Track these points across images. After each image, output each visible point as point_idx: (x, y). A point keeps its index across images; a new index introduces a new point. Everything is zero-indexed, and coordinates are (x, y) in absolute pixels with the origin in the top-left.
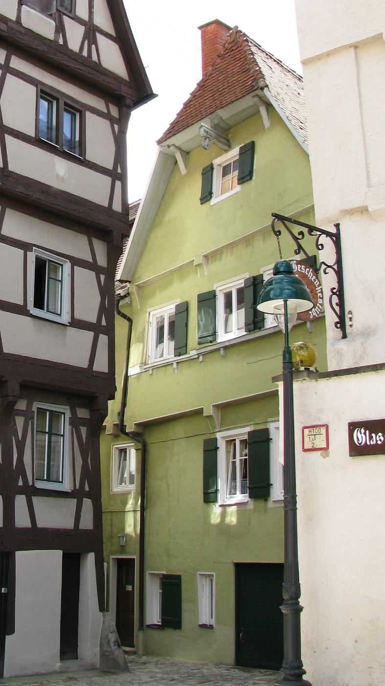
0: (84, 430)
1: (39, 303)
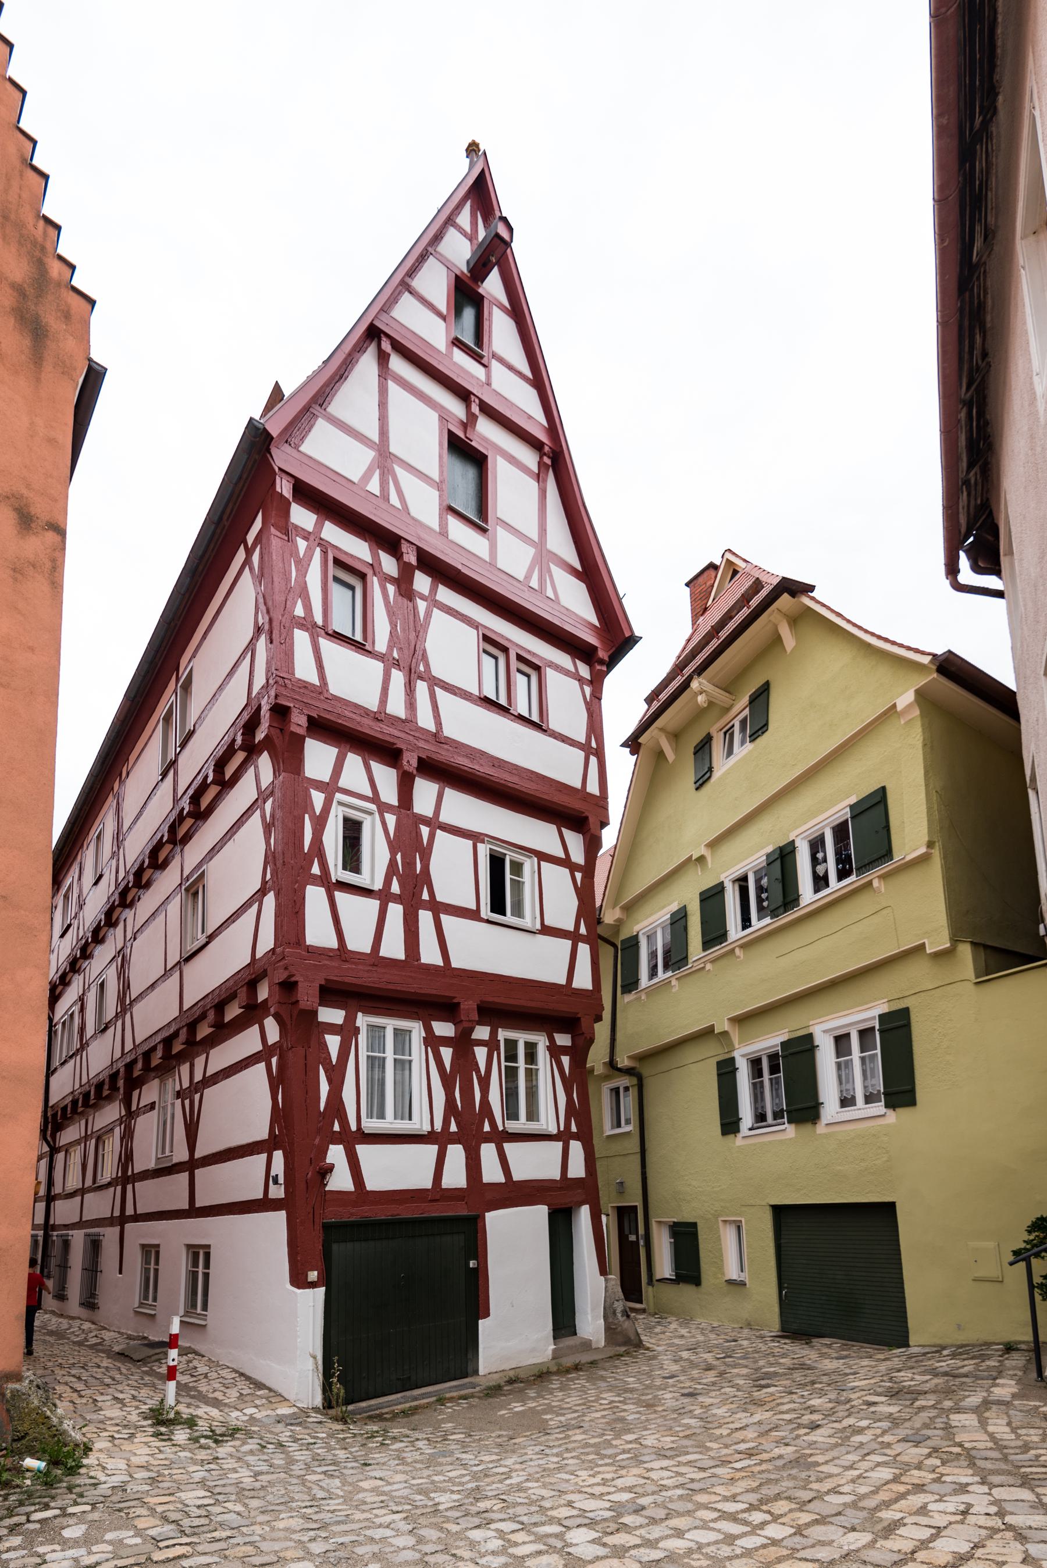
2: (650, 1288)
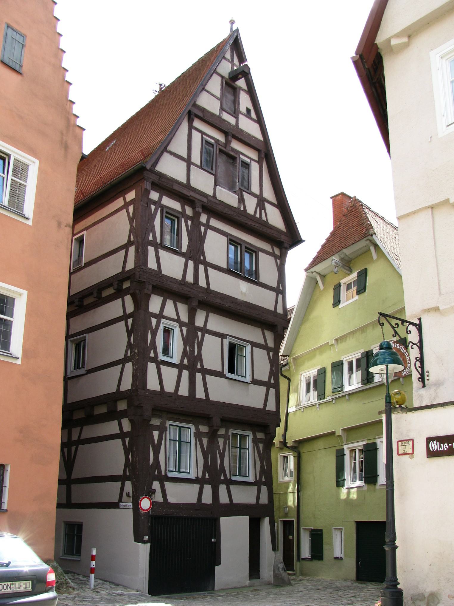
0: (261, 446)
1: (231, 370)
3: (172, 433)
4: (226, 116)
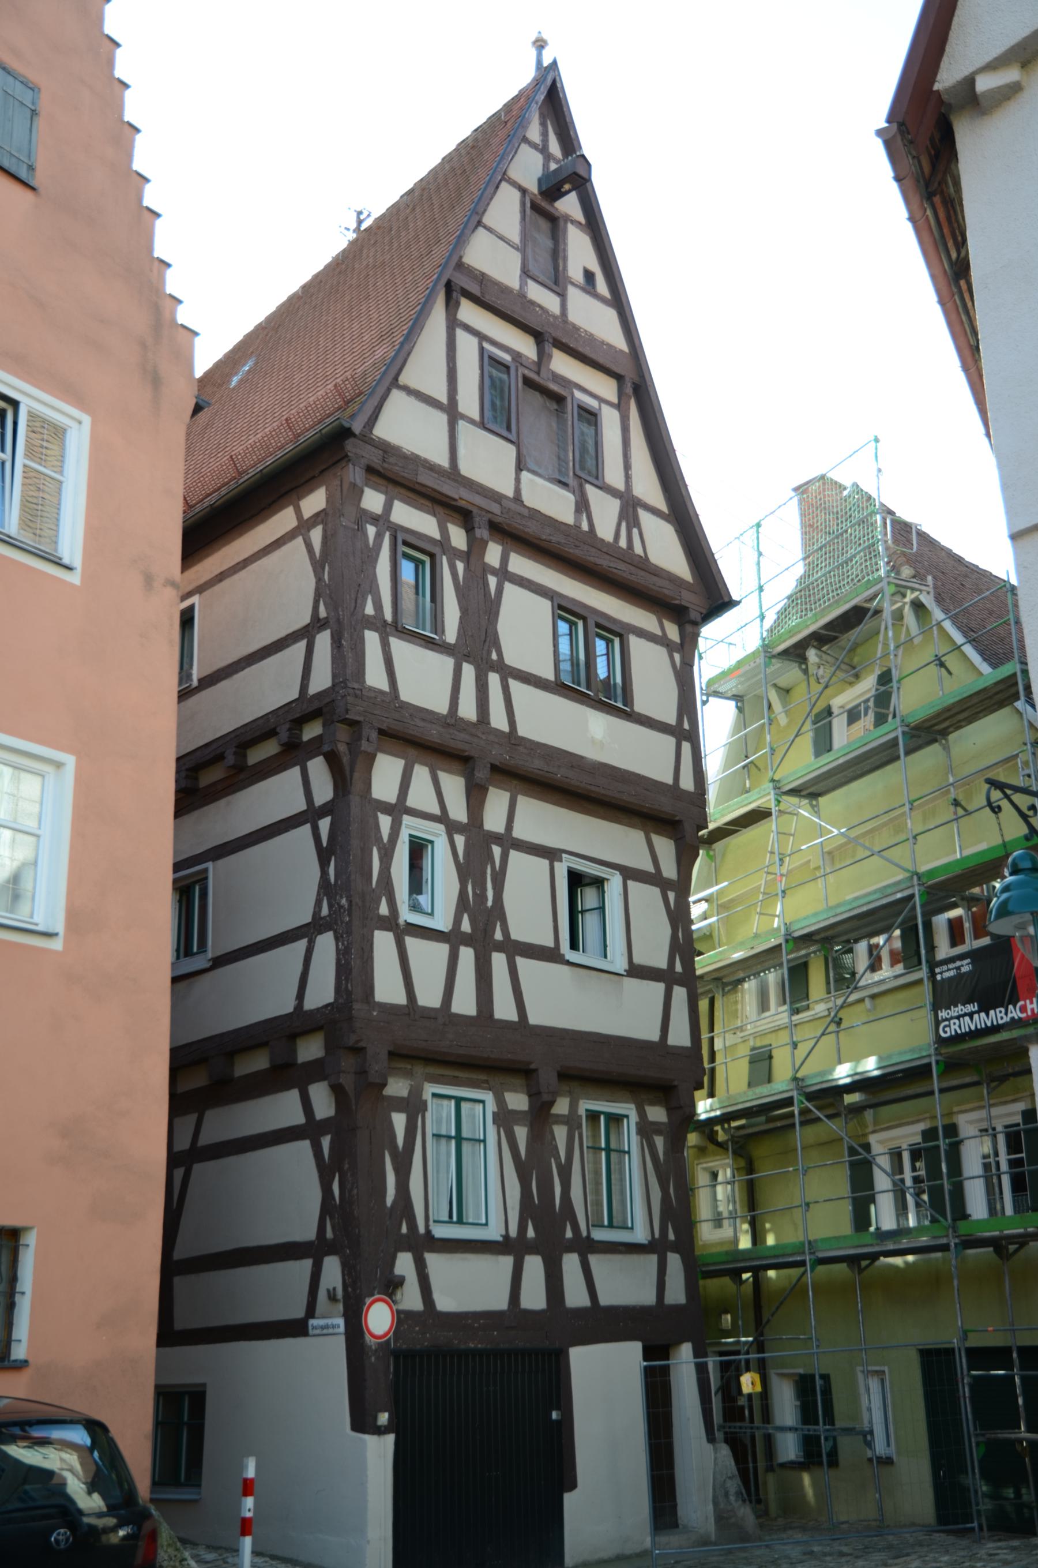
0: (659, 1141)
2: (771, 1478)
3: (439, 1116)
4: (537, 293)
